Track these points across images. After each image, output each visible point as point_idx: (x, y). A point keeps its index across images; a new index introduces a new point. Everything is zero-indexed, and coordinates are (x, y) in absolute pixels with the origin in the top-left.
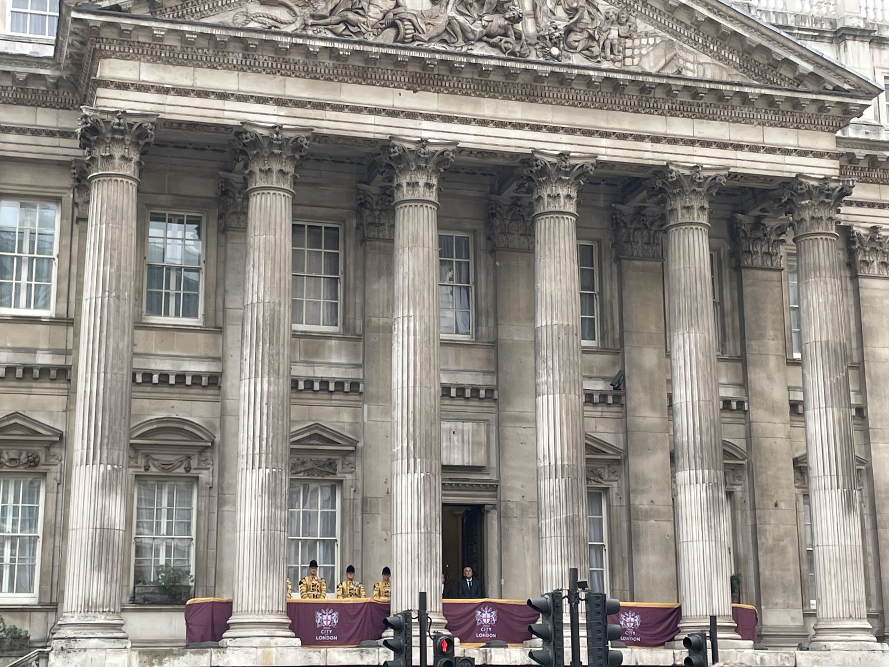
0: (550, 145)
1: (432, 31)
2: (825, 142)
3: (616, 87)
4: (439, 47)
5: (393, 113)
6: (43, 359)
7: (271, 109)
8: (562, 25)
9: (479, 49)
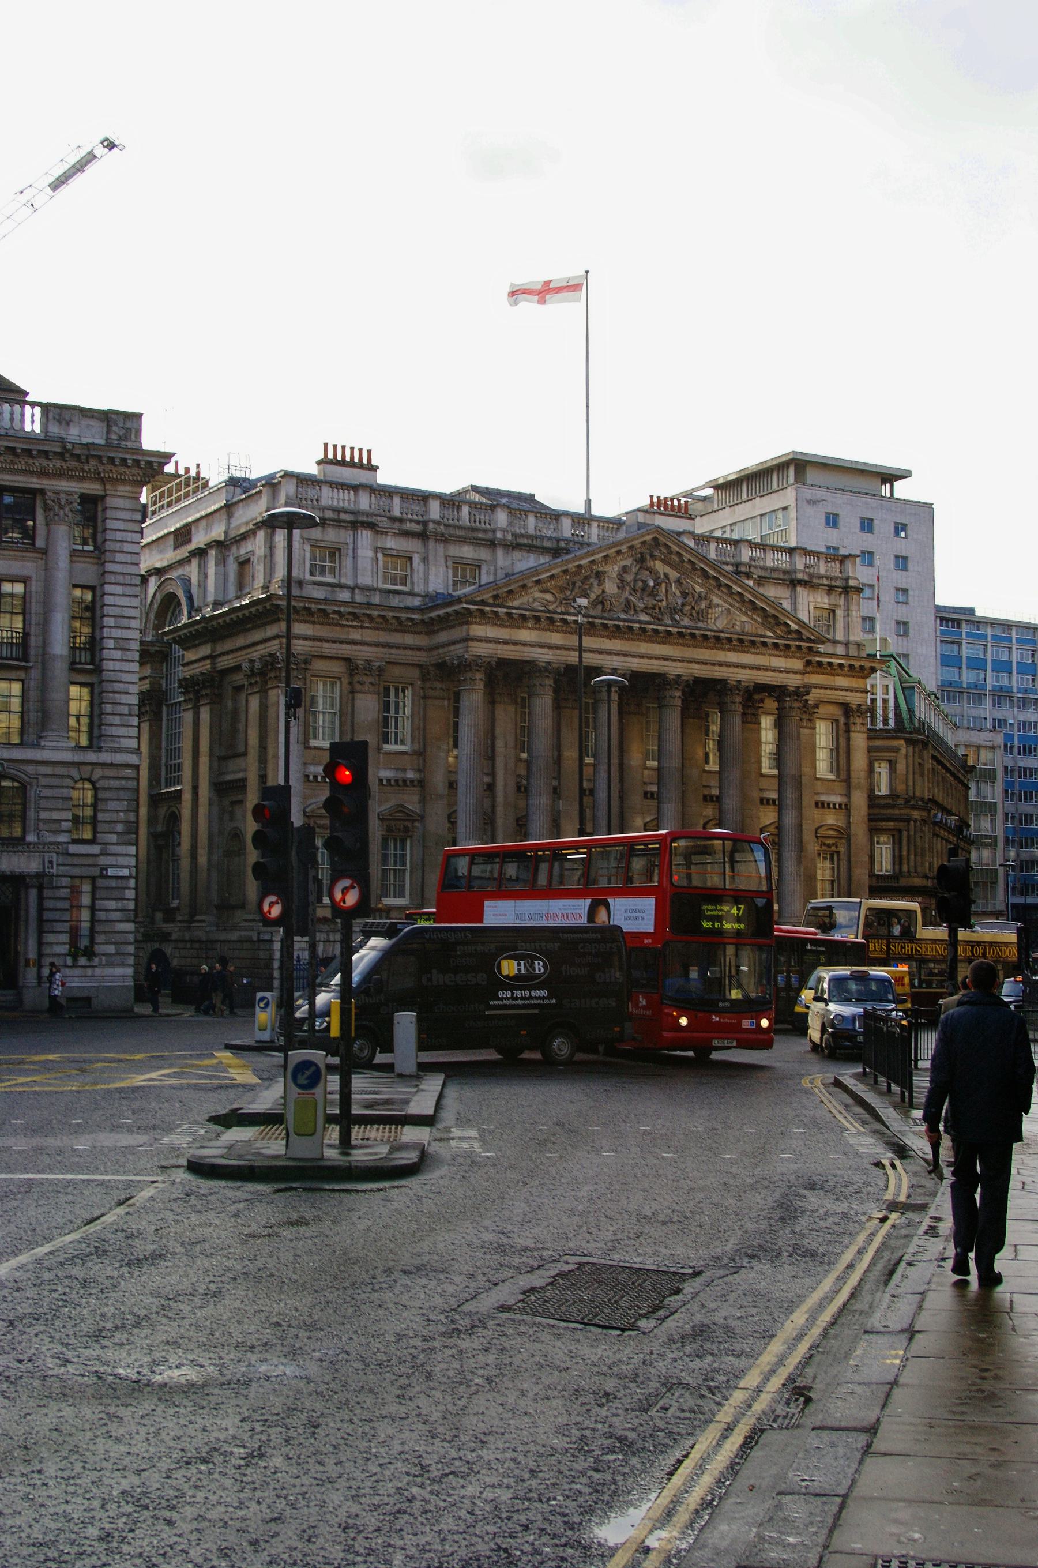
0: (674, 669)
2: (798, 664)
3: (705, 637)
4: (623, 616)
6: (410, 775)
7: (545, 651)
8: (680, 601)
9: (644, 617)
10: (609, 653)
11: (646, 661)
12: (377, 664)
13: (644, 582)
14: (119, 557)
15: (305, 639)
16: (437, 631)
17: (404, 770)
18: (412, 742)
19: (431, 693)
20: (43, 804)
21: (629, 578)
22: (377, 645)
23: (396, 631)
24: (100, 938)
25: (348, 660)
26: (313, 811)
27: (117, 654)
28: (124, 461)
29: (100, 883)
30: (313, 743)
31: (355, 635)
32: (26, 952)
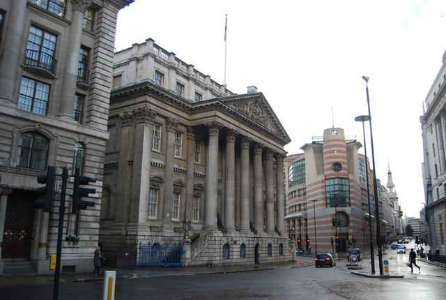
6: (182, 168)
14: (106, 36)
17: (180, 166)
18: (182, 155)
20: (59, 152)
24: (82, 231)
25: (165, 118)
27: (102, 82)
31: (170, 108)
32: (40, 238)
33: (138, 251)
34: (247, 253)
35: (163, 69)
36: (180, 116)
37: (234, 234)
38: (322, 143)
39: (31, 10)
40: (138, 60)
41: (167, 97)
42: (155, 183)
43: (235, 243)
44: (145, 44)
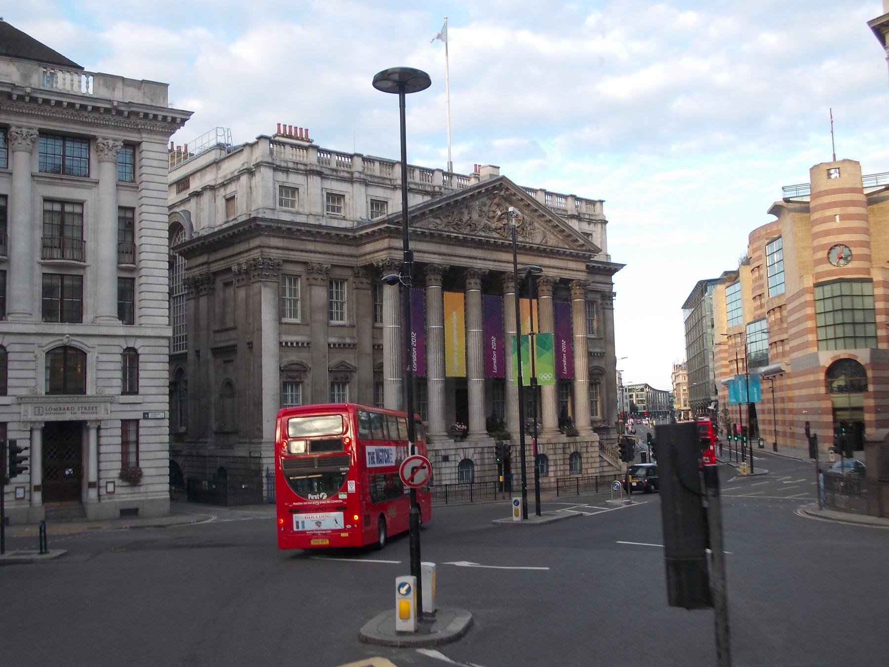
1: (480, 227)
2: (583, 266)
5: (471, 258)
6: (348, 341)
10: (475, 258)
11: (497, 264)
12: (325, 266)
13: (494, 212)
14: (152, 186)
15: (278, 248)
16: (365, 244)
17: (344, 338)
18: (349, 317)
19: (360, 286)
21: (485, 209)
22: (325, 253)
23: (337, 244)
25: (306, 263)
26: (286, 366)
28: (155, 116)
29: (142, 423)
30: (284, 320)
31: (311, 246)
33: (265, 480)
34: (476, 474)
35: (294, 180)
36: (333, 254)
37: (442, 444)
38: (807, 199)
39: (38, 182)
40: (250, 172)
41: (298, 230)
42: (291, 374)
43: (446, 459)
44: (257, 143)
